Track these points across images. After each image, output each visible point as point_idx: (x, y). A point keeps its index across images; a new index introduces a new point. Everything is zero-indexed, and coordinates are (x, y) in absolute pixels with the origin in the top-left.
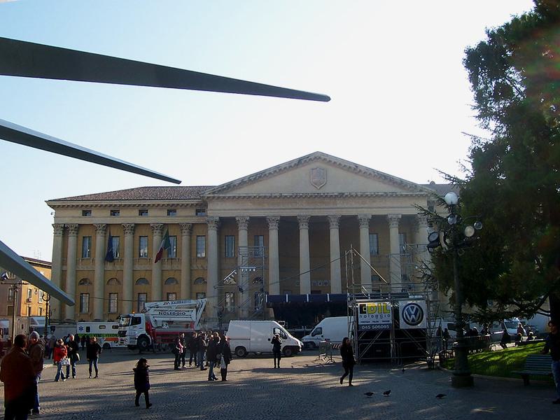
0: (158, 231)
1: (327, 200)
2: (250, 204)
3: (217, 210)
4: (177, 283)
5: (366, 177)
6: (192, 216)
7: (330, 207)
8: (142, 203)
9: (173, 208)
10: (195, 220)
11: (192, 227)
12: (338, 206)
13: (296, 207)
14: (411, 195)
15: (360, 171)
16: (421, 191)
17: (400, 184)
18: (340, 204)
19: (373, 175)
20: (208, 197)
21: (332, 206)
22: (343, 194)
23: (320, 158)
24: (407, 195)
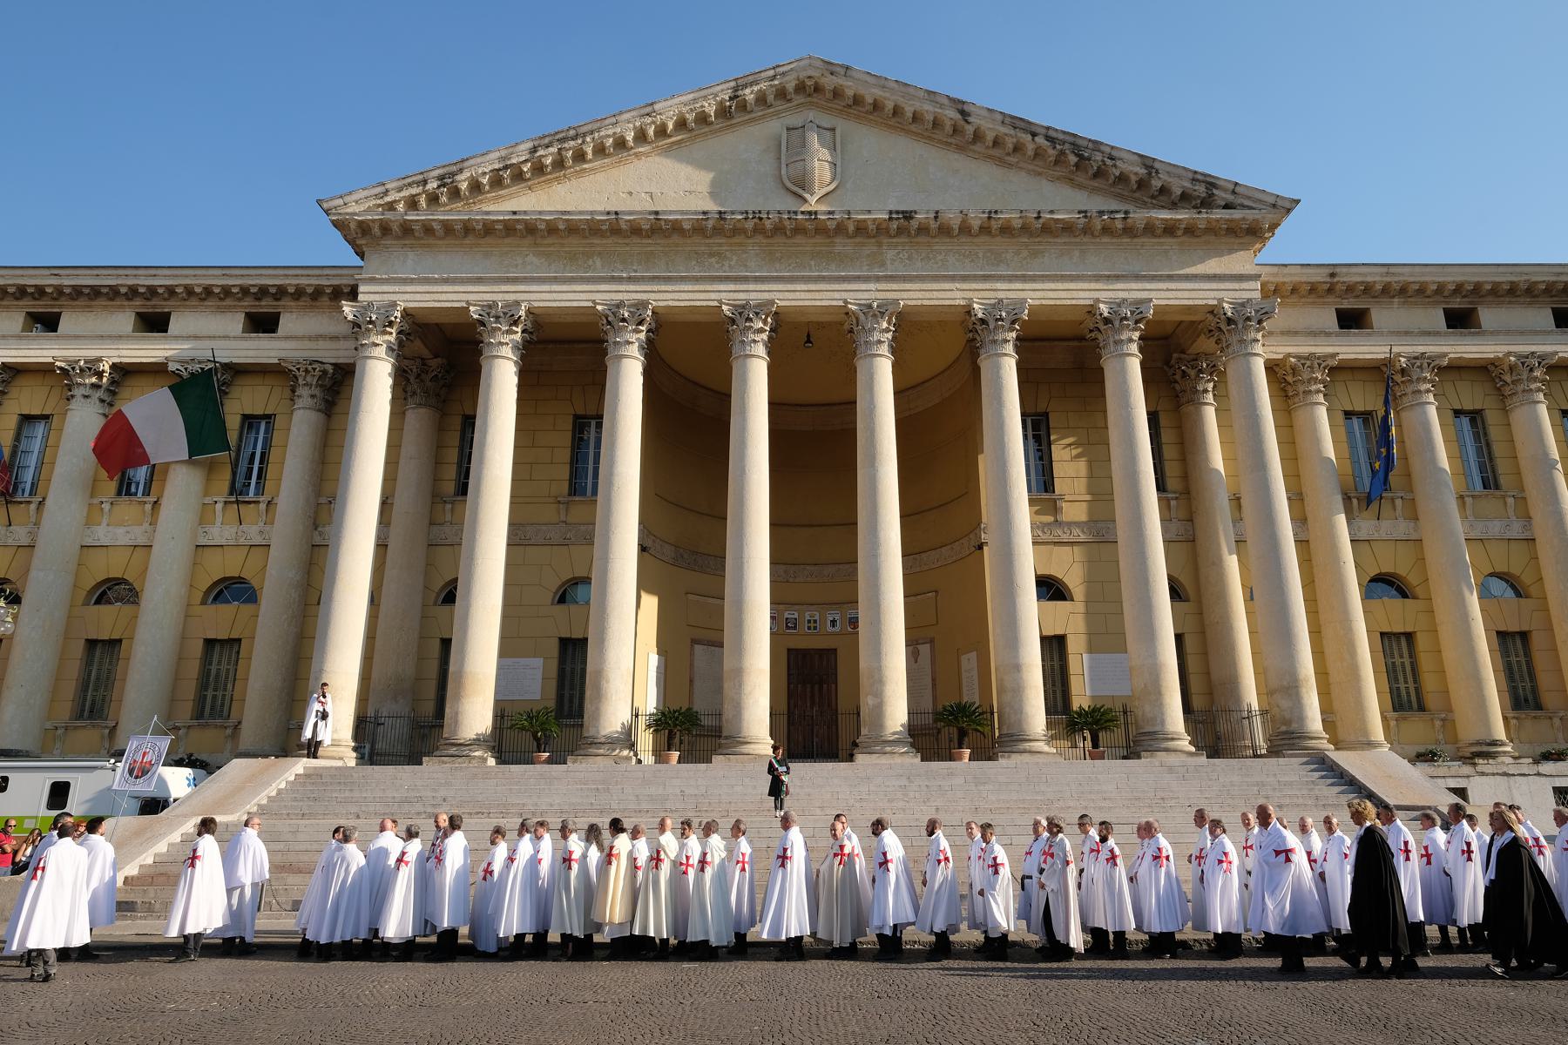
1: (841, 245)
2: (531, 258)
5: (1001, 162)
15: (978, 136)
16: (1227, 207)
17: (1142, 184)
19: (1030, 147)
22: (908, 216)
23: (818, 89)
24: (1170, 230)
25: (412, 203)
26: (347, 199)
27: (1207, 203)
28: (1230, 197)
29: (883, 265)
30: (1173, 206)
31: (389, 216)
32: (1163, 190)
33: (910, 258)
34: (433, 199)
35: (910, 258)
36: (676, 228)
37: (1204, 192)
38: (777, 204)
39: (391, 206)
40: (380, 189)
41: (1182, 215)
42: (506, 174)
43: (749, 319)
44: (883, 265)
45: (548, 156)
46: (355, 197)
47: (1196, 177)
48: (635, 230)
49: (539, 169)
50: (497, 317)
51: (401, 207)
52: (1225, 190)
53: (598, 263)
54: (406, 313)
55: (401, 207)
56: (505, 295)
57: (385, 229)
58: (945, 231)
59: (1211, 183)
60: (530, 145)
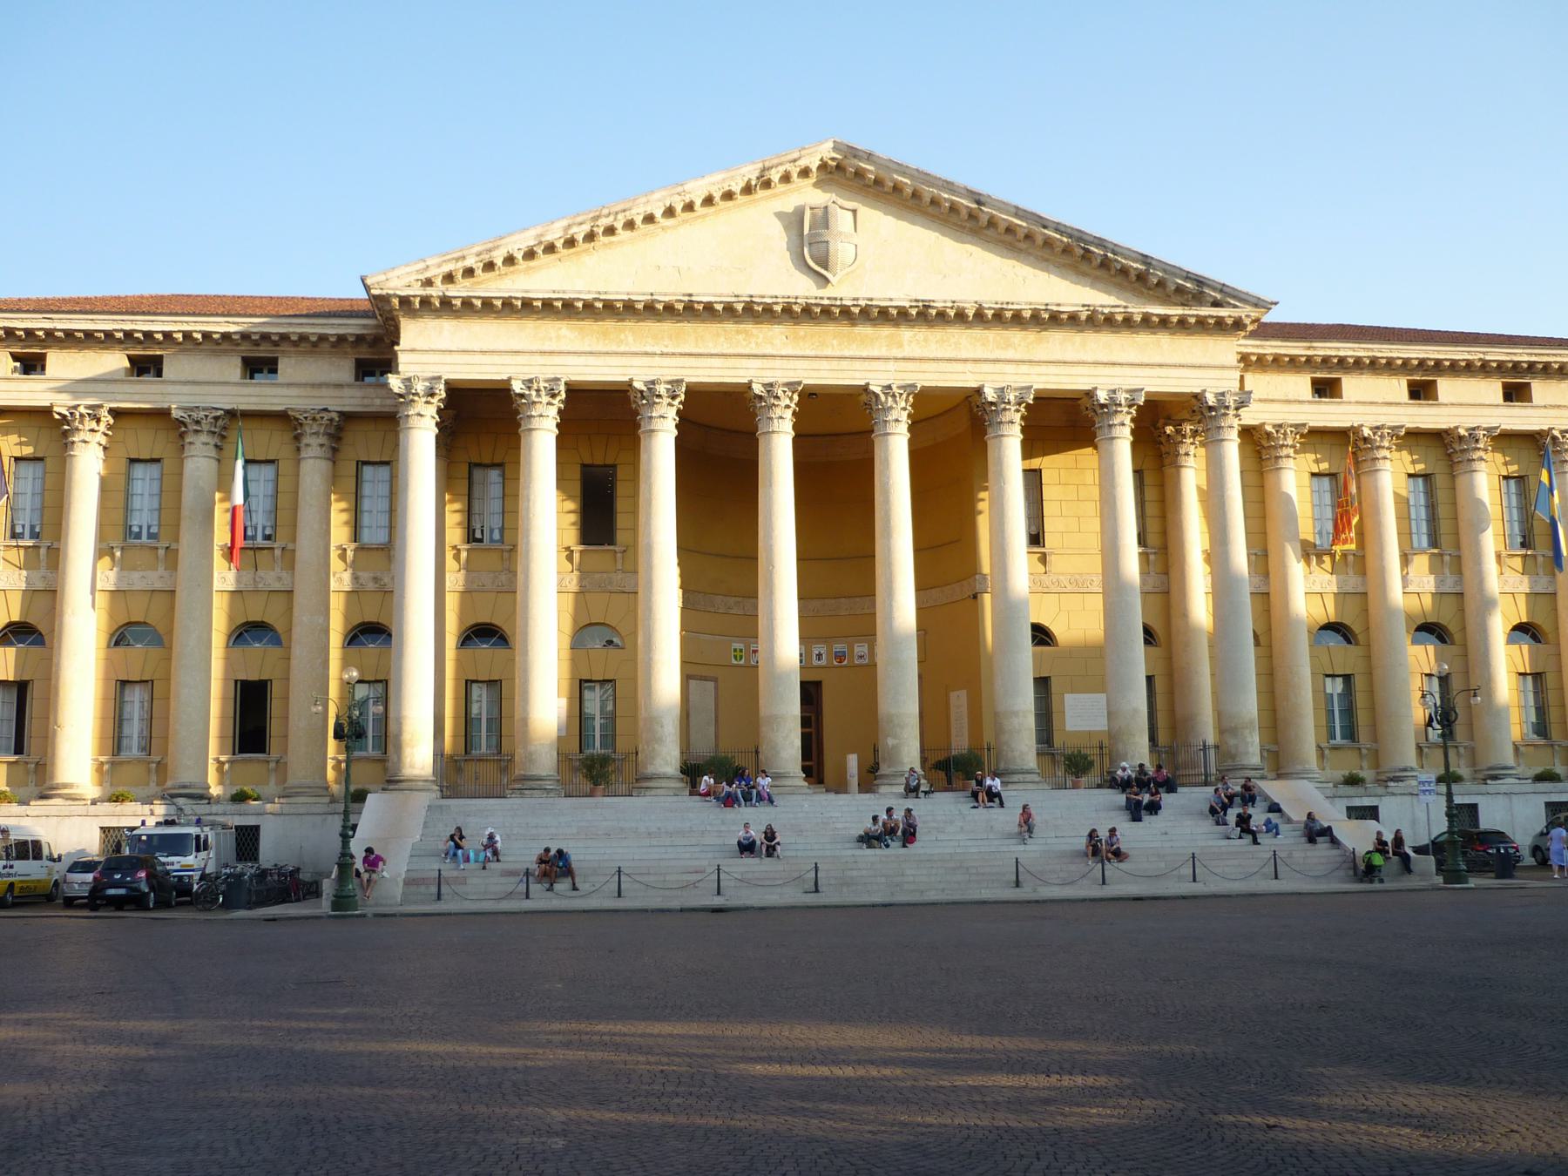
0: (204, 438)
3: (432, 355)
4: (277, 641)
6: (339, 386)
7: (876, 353)
8: (140, 324)
9: (264, 351)
10: (354, 399)
11: (342, 427)
12: (907, 353)
13: (747, 351)
14: (1182, 323)
18: (912, 339)
20: (405, 301)
21: (883, 352)
24: (1164, 322)
25: (449, 278)
26: (390, 275)
27: (1198, 298)
28: (1218, 296)
29: (900, 345)
30: (1166, 300)
31: (429, 291)
32: (1161, 284)
33: (926, 340)
34: (469, 272)
35: (926, 340)
36: (709, 307)
37: (1195, 290)
38: (802, 289)
39: (428, 283)
40: (421, 265)
41: (1175, 311)
42: (539, 250)
43: (777, 397)
44: (900, 345)
45: (580, 232)
46: (397, 272)
47: (1188, 276)
48: (669, 309)
49: (570, 243)
50: (538, 391)
51: (438, 281)
52: (1214, 289)
53: (630, 339)
54: (447, 383)
55: (438, 281)
56: (539, 362)
57: (426, 302)
58: (961, 316)
59: (1200, 282)
60: (565, 223)
